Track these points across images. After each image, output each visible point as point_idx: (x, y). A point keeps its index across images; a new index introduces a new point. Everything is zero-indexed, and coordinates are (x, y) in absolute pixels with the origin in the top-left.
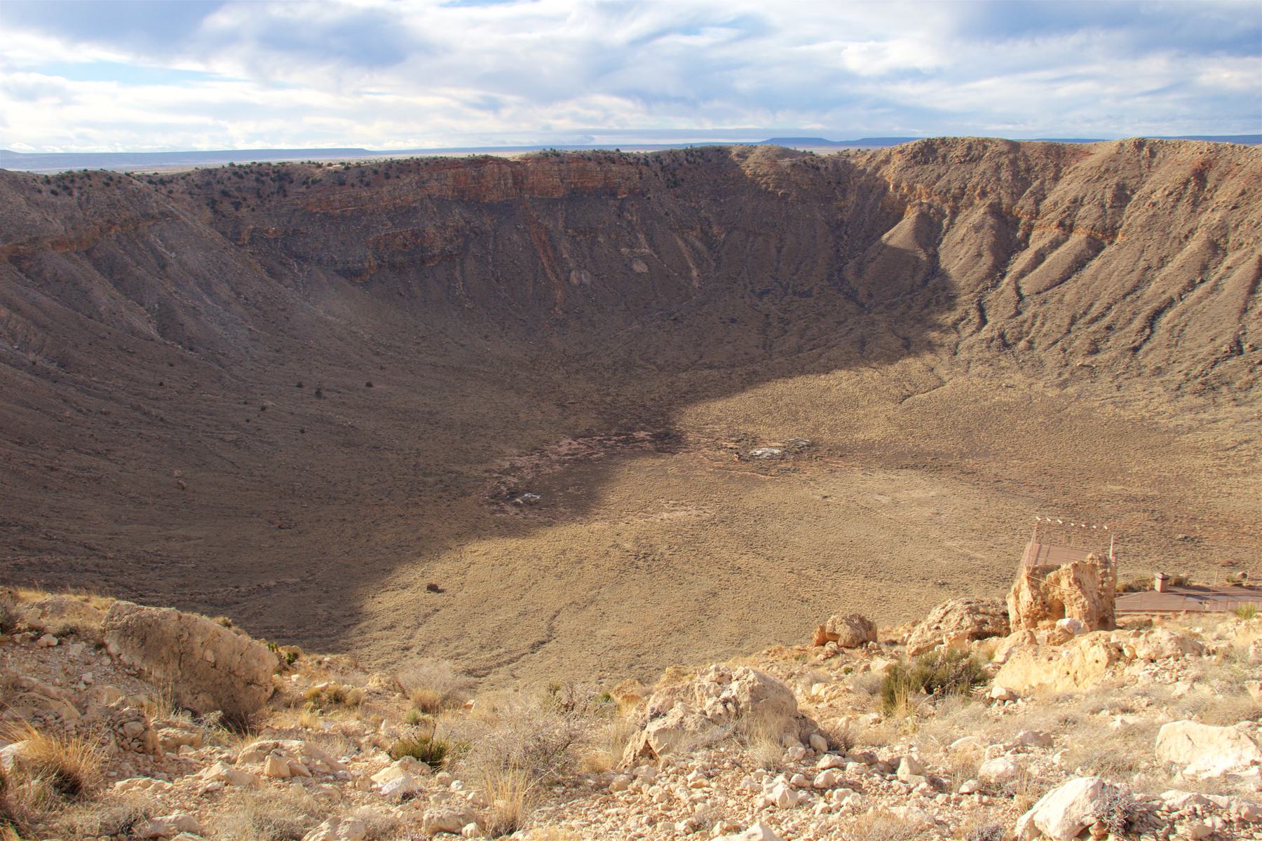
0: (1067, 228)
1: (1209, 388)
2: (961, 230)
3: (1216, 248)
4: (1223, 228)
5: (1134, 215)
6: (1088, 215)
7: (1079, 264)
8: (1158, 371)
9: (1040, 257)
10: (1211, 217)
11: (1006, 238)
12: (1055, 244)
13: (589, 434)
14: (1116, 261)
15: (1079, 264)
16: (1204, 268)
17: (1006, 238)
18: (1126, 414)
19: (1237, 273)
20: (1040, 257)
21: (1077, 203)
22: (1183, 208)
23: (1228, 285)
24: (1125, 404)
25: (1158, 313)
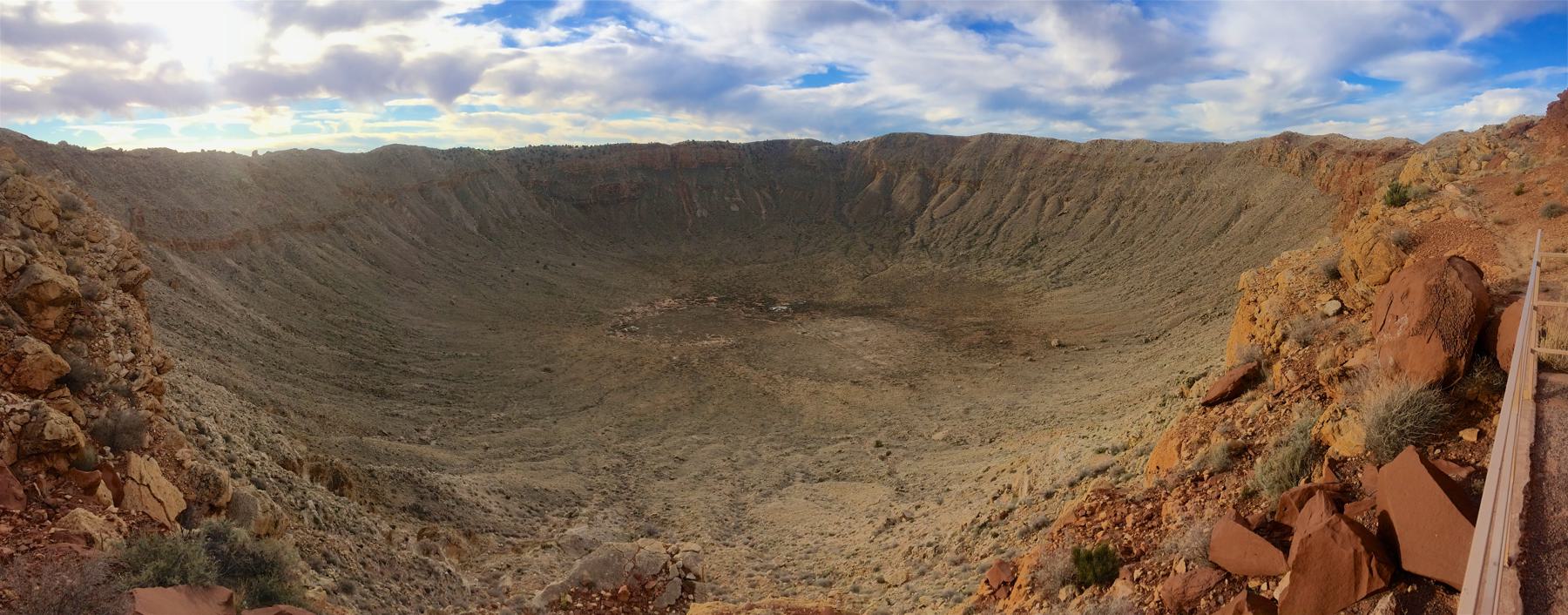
0: (957, 182)
1: (1022, 262)
2: (903, 185)
3: (1025, 190)
4: (1026, 179)
5: (988, 175)
6: (967, 175)
7: (962, 202)
8: (1000, 255)
9: (943, 199)
10: (1021, 174)
11: (927, 190)
12: (952, 191)
13: (684, 296)
14: (980, 201)
15: (962, 202)
16: (1020, 201)
17: (927, 190)
18: (982, 279)
19: (1034, 202)
20: (943, 199)
21: (962, 168)
22: (1009, 170)
23: (1030, 208)
24: (982, 273)
25: (1000, 225)
